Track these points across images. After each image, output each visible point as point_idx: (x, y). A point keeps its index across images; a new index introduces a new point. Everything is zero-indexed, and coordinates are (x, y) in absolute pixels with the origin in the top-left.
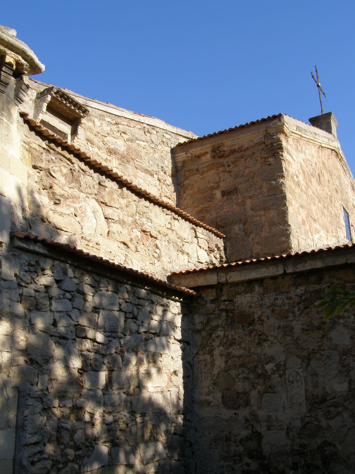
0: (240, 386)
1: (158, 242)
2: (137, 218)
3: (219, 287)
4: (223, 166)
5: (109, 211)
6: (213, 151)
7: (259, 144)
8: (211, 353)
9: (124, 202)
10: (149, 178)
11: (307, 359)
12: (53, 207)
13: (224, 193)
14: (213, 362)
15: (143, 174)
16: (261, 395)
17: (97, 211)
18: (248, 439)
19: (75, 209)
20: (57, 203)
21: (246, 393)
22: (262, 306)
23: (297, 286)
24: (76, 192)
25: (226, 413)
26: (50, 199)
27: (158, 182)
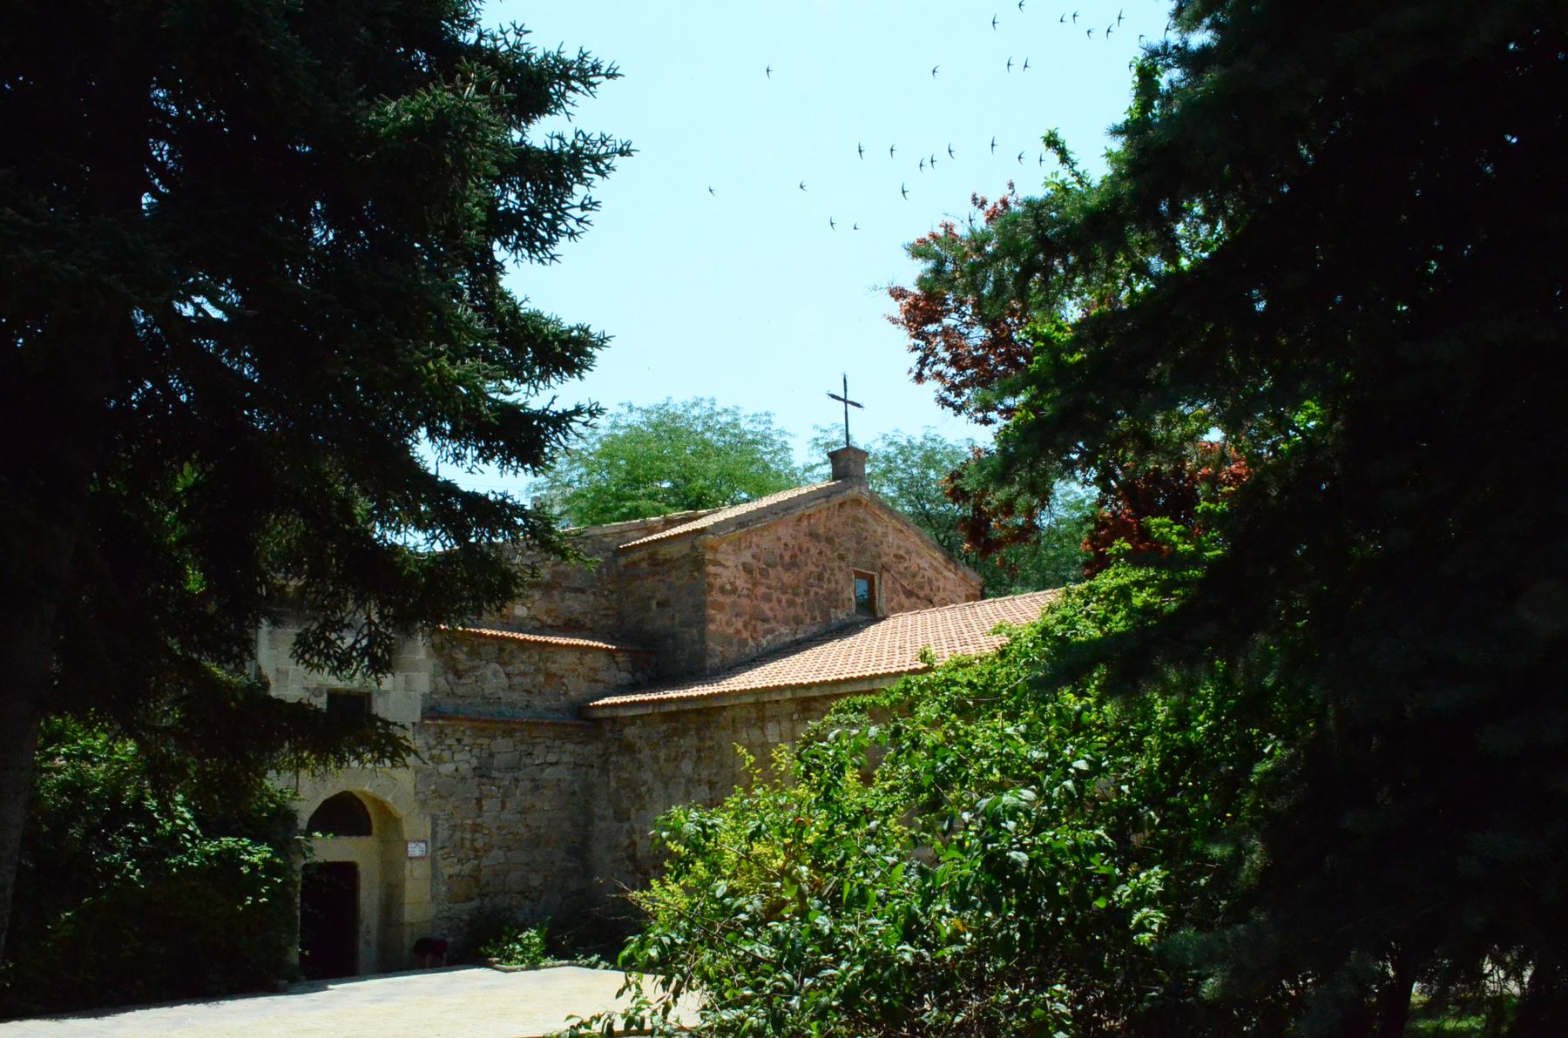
0: (626, 804)
1: (565, 680)
2: (541, 665)
3: (613, 720)
4: (658, 574)
5: (510, 669)
6: (650, 558)
7: (688, 555)
8: (608, 776)
9: (524, 657)
10: (583, 597)
11: (666, 785)
12: (457, 681)
13: (658, 604)
14: (608, 783)
15: (573, 595)
16: (637, 811)
17: (498, 672)
18: (628, 846)
19: (477, 677)
20: (460, 677)
21: (629, 810)
22: (640, 738)
23: (664, 722)
24: (476, 663)
25: (616, 825)
26: (455, 675)
27: (592, 597)
